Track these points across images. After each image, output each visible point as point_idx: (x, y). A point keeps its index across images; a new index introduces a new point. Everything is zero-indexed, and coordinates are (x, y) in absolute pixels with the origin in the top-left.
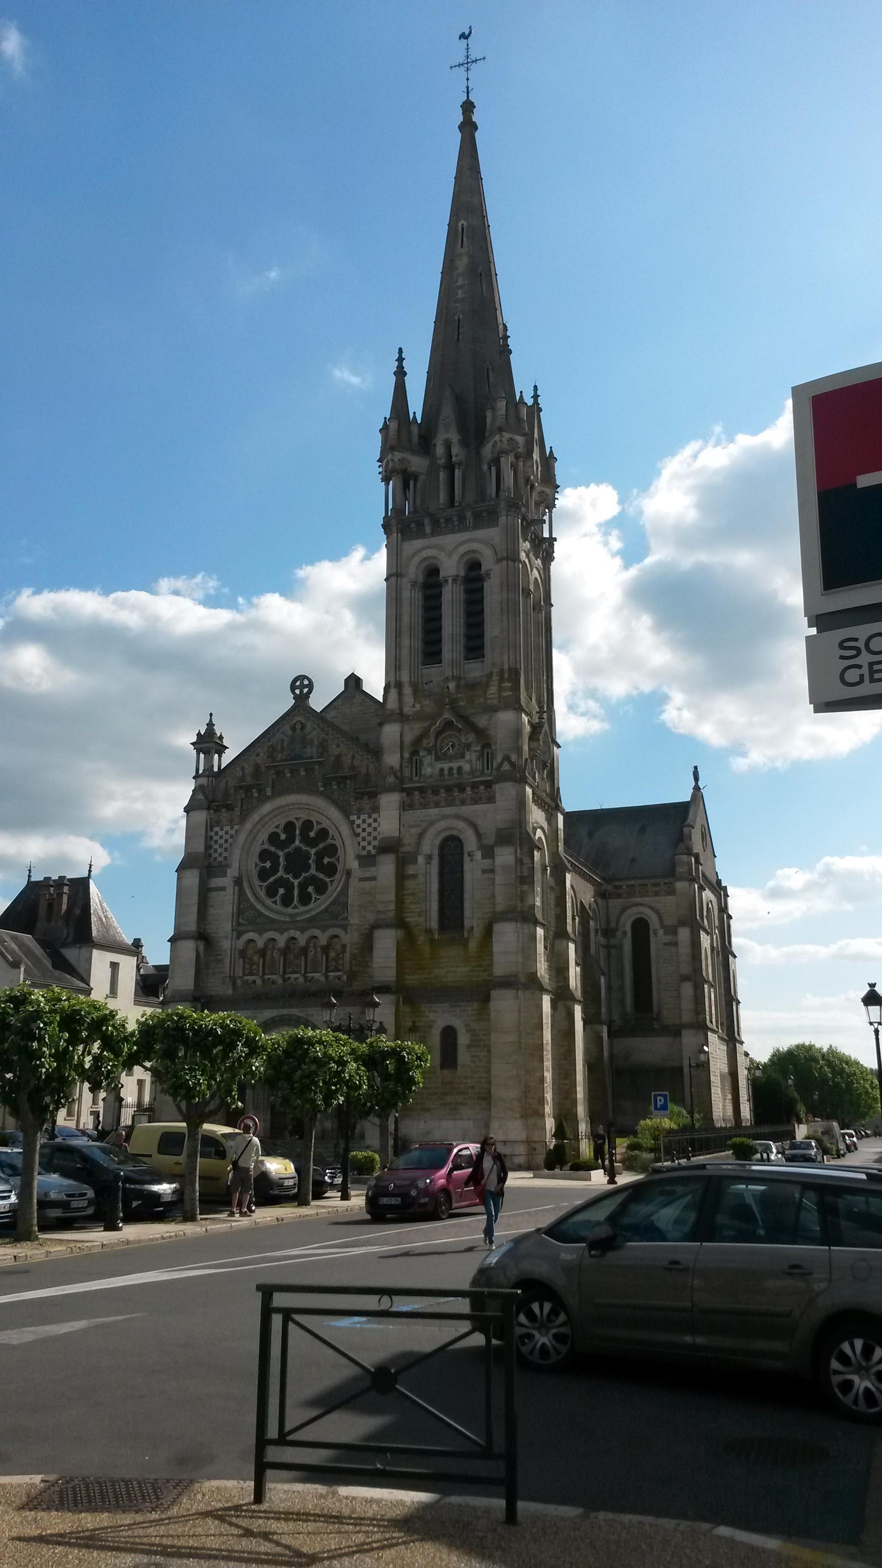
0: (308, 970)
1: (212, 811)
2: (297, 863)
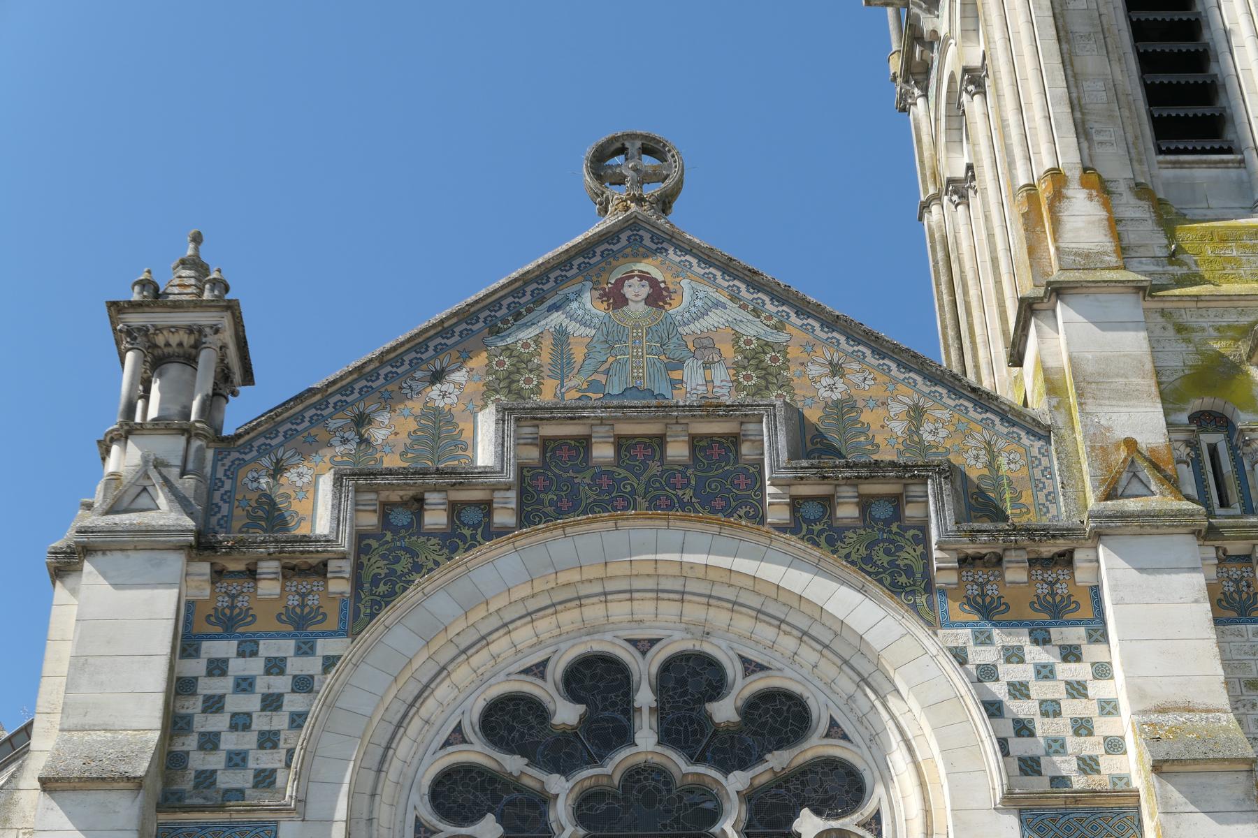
1: (205, 568)
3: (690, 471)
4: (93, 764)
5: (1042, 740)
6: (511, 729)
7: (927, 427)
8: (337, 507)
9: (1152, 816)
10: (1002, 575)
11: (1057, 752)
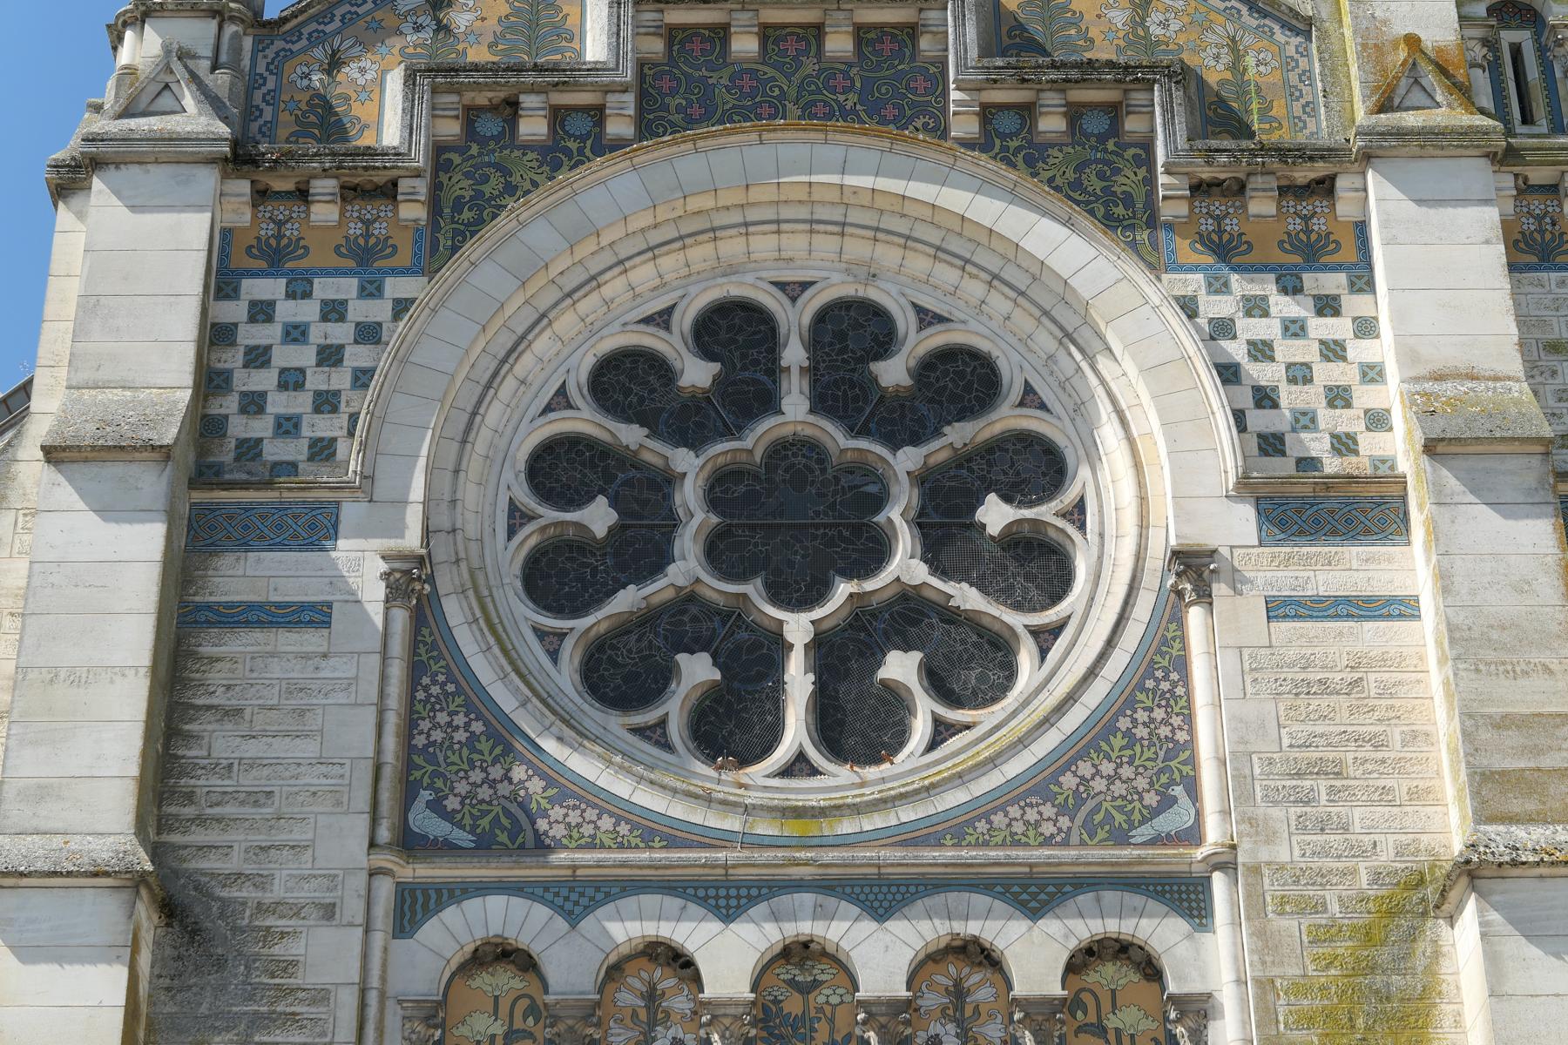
1: (244, 187)
3: (855, 70)
4: (108, 429)
5: (1287, 413)
6: (627, 392)
7: (1155, 17)
8: (409, 111)
9: (1421, 507)
10: (1244, 207)
11: (1305, 427)
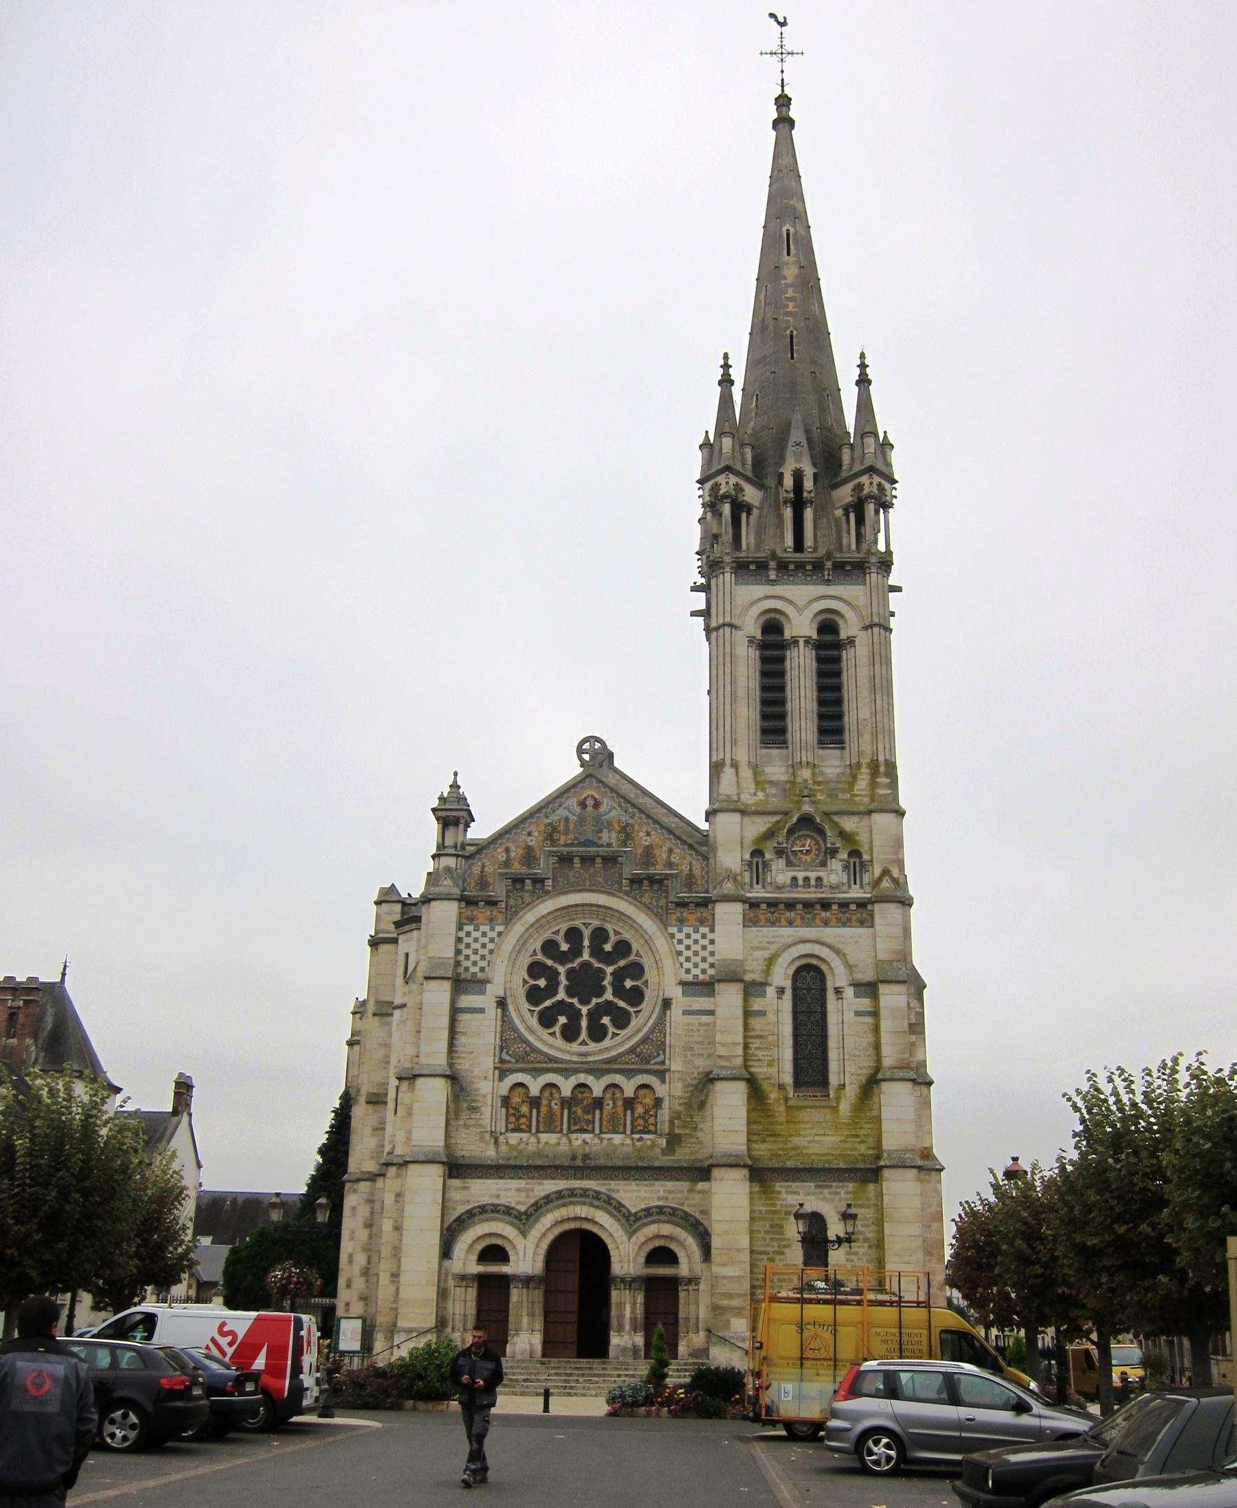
0: (604, 1130)
2: (584, 982)
